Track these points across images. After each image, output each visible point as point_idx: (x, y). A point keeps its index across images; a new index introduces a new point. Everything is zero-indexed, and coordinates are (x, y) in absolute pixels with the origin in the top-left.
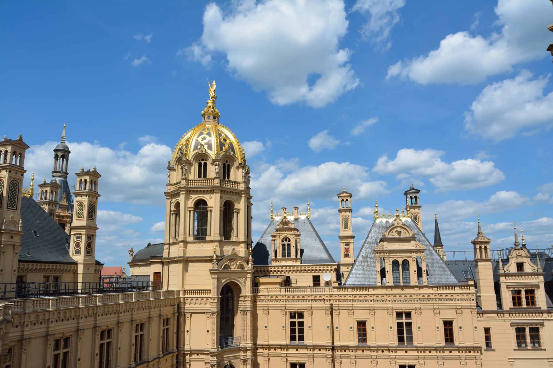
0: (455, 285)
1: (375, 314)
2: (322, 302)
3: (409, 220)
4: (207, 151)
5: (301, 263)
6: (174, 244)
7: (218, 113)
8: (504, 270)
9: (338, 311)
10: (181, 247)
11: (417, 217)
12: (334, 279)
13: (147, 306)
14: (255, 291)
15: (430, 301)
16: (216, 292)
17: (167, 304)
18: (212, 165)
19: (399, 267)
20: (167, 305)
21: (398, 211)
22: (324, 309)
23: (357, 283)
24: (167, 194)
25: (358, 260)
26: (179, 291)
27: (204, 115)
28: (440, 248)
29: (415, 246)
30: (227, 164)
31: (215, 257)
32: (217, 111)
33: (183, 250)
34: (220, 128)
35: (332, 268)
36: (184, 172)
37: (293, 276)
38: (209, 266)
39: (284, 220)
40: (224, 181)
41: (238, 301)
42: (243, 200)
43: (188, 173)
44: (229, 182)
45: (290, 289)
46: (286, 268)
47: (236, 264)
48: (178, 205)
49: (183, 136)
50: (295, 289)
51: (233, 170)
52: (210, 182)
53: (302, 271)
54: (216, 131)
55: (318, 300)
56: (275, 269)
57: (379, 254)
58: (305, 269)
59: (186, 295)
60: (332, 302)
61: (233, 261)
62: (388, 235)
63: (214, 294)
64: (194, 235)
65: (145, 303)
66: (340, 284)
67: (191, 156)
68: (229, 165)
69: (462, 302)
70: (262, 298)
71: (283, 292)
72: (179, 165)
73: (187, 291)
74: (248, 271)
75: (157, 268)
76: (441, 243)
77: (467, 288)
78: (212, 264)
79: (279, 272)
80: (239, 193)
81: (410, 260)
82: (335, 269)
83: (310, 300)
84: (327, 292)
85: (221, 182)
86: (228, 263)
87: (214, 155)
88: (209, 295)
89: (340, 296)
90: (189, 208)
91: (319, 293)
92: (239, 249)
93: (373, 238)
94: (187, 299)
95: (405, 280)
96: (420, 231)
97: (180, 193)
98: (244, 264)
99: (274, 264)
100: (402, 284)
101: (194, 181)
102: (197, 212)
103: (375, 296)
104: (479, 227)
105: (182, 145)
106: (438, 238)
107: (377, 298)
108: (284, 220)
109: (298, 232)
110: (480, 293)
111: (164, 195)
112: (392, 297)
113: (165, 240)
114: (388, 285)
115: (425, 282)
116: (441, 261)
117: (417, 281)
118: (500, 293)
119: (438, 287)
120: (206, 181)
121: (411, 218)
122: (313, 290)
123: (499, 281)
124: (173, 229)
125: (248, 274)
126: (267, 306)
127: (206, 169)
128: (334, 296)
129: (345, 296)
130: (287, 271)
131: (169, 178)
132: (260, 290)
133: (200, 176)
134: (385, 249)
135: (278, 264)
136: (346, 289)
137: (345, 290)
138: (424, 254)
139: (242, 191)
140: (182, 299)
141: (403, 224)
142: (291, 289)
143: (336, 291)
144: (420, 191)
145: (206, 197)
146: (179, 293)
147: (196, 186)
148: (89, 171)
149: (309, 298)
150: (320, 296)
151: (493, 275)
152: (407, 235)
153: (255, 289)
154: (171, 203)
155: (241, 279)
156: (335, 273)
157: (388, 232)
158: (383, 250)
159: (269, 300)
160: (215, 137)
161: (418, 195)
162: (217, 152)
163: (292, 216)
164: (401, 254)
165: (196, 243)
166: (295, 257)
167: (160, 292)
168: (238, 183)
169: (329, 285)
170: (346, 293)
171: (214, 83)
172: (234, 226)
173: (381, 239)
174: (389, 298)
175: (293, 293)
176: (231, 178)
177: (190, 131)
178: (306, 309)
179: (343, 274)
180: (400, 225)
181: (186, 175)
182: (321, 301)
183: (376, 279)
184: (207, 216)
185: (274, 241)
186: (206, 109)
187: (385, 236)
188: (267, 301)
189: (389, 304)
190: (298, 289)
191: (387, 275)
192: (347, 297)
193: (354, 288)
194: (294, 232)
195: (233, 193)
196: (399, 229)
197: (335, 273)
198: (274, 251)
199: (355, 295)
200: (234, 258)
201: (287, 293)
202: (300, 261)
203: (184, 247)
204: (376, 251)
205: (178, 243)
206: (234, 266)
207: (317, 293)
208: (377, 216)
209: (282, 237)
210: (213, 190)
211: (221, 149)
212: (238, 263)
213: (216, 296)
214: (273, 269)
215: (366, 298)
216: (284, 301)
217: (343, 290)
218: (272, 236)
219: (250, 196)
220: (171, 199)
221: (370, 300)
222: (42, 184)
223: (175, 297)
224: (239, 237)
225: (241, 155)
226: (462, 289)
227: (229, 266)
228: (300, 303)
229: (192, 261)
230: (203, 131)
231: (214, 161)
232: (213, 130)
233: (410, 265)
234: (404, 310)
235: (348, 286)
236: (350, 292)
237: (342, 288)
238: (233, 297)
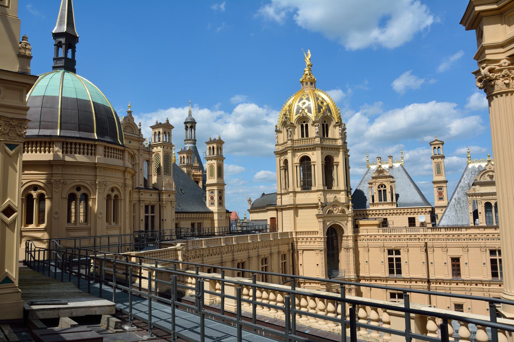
1: (468, 251)
2: (417, 241)
5: (397, 206)
6: (285, 194)
9: (432, 249)
10: (291, 197)
12: (429, 221)
14: (356, 231)
18: (313, 126)
21: (490, 156)
22: (419, 247)
23: (450, 224)
24: (276, 153)
25: (451, 203)
26: (292, 232)
27: (302, 82)
30: (325, 124)
31: (320, 204)
32: (313, 77)
35: (426, 211)
36: (290, 133)
37: (390, 218)
38: (316, 211)
39: (379, 169)
41: (342, 240)
42: (341, 154)
45: (387, 229)
46: (383, 211)
47: (338, 209)
48: (286, 162)
49: (286, 102)
50: (391, 230)
51: (331, 128)
52: (311, 141)
53: (398, 213)
54: (314, 96)
56: (373, 213)
57: (471, 197)
58: (401, 212)
60: (426, 241)
61: (335, 206)
63: (321, 235)
64: (301, 186)
66: (433, 225)
67: (294, 120)
68: (327, 125)
70: (362, 237)
73: (299, 232)
75: (273, 214)
79: (377, 215)
80: (337, 149)
82: (429, 211)
83: (406, 239)
84: (421, 231)
86: (331, 209)
89: (433, 235)
90: (295, 164)
91: (414, 233)
93: (466, 182)
94: (299, 239)
97: (287, 151)
99: (371, 208)
101: (298, 141)
103: (468, 235)
105: (286, 110)
107: (470, 237)
109: (393, 179)
112: (485, 236)
114: (480, 225)
120: (309, 140)
122: (409, 230)
125: (349, 218)
126: (367, 244)
130: (384, 214)
131: (277, 140)
132: (360, 230)
133: (303, 136)
134: (477, 192)
135: (375, 208)
136: (440, 229)
137: (439, 230)
139: (340, 146)
140: (295, 239)
142: (388, 230)
143: (429, 231)
145: (309, 154)
146: (292, 234)
147: (300, 145)
148: (215, 139)
149: (405, 238)
150: (415, 235)
153: (356, 230)
154: (280, 160)
156: (429, 215)
157: (480, 176)
158: (475, 194)
159: (369, 240)
160: (313, 101)
162: (316, 115)
166: (391, 201)
168: (336, 140)
169: (424, 226)
170: (439, 233)
171: (309, 52)
172: (335, 177)
173: (474, 183)
174: (482, 237)
175: (390, 233)
176: (330, 136)
177: (291, 98)
178: (402, 247)
179: (437, 215)
181: (291, 136)
182: (416, 240)
183: (468, 220)
185: (371, 187)
186: (304, 77)
187: (477, 180)
188: (367, 240)
189: (482, 243)
191: (480, 216)
192: (441, 237)
194: (389, 179)
196: (491, 173)
198: (371, 196)
199: (448, 235)
200: (336, 204)
201: (384, 233)
202: (396, 204)
203: (293, 197)
204: (468, 194)
205: (288, 193)
206: (337, 211)
207: (412, 233)
208: (470, 162)
209: (378, 184)
210: (315, 148)
211: (320, 111)
212: (340, 208)
213: (322, 236)
214: (371, 212)
215: (459, 237)
216: (382, 240)
217: (436, 230)
218: (368, 183)
219: (347, 149)
221: (463, 239)
222: (180, 152)
223: (289, 237)
225: (337, 115)
228: (396, 241)
229: (301, 208)
230: (303, 97)
231: (314, 122)
232: (311, 95)
234: (497, 248)
235: (442, 226)
236: (443, 231)
237: (436, 229)
238: (337, 237)
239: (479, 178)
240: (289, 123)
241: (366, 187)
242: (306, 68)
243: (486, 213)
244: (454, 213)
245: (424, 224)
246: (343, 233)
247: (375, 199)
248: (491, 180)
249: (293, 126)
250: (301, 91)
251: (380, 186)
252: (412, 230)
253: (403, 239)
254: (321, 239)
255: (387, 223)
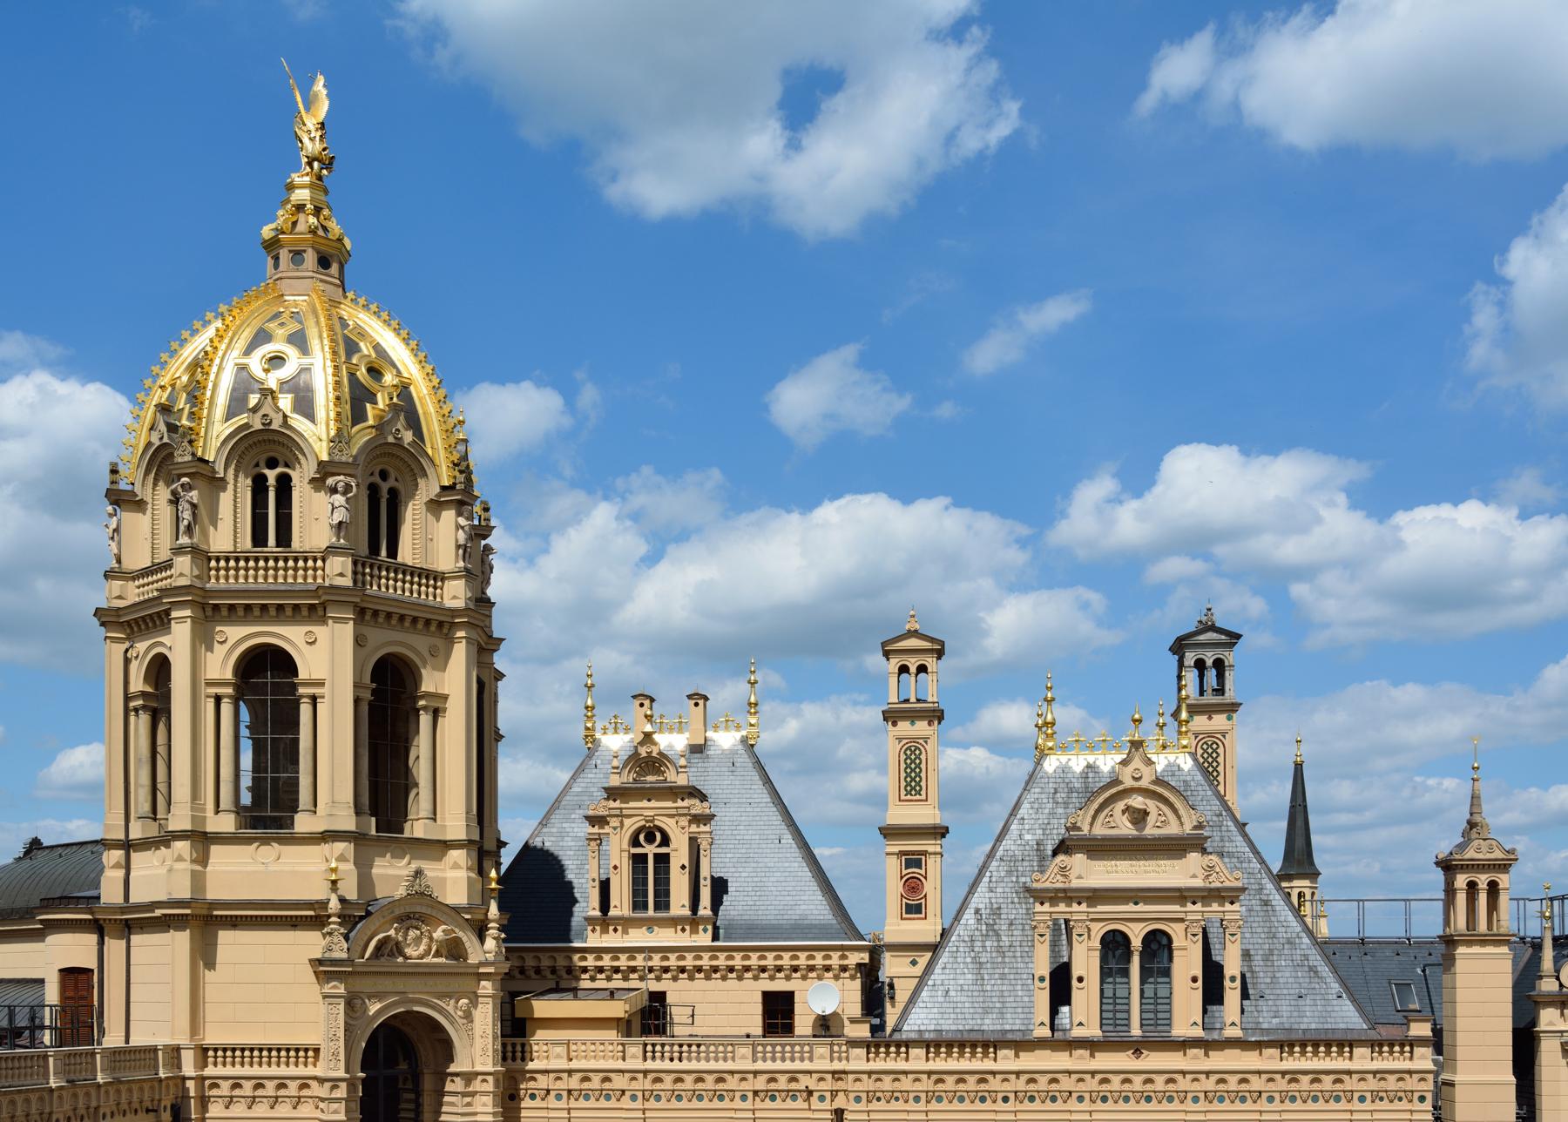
0: (1356, 1037)
2: (800, 1104)
3: (1186, 763)
4: (291, 422)
5: (715, 937)
6: (146, 844)
7: (340, 240)
8: (1558, 978)
10: (180, 859)
11: (1221, 751)
12: (855, 1009)
13: (33, 1111)
15: (1249, 1101)
16: (342, 1057)
17: (124, 1106)
18: (317, 490)
19: (1128, 961)
20: (125, 1107)
21: (1140, 721)
23: (950, 1025)
24: (108, 618)
25: (959, 930)
26: (177, 1050)
27: (272, 246)
28: (1307, 883)
29: (1201, 874)
30: (384, 487)
31: (334, 905)
32: (335, 228)
33: (192, 871)
34: (350, 315)
35: (845, 962)
36: (187, 515)
37: (677, 993)
38: (312, 943)
39: (643, 751)
40: (371, 567)
41: (441, 1093)
42: (460, 653)
43: (206, 520)
44: (396, 572)
45: (663, 1045)
46: (650, 958)
47: (431, 938)
48: (160, 669)
50: (685, 1048)
51: (413, 514)
52: (306, 569)
53: (715, 969)
54: (331, 328)
55: (784, 1094)
56: (600, 963)
57: (1047, 905)
58: (730, 963)
59: (211, 1067)
60: (840, 1102)
61: (415, 923)
62: (1092, 824)
63: (333, 1065)
64: (239, 809)
65: (27, 1101)
66: (876, 1029)
67: (215, 444)
68: (393, 493)
69: (1379, 1105)
70: (543, 1082)
71: (634, 1057)
72: (161, 484)
73: (216, 1050)
74: (482, 970)
75: (76, 949)
76: (1312, 863)
77: (1402, 1052)
78: (324, 936)
79: (619, 976)
80: (440, 625)
81: (1176, 932)
82: (859, 965)
83: (750, 1095)
84: (822, 1058)
85: (360, 568)
86: (392, 932)
87: (325, 444)
88: (310, 1067)
90: (210, 684)
91: (788, 1065)
92: (440, 874)
93: (1028, 837)
94: (216, 1086)
95: (1151, 1016)
96: (1228, 809)
97: (167, 612)
98: (465, 939)
99: (594, 939)
100: (1136, 1031)
101: (232, 563)
102: (248, 703)
103: (1024, 1078)
104: (1475, 799)
105: (173, 386)
106: (1300, 842)
107: (1032, 1087)
108: (643, 751)
109: (706, 804)
110: (1454, 1072)
111: (96, 622)
112: (1092, 1084)
113: (107, 828)
114: (1077, 1032)
115: (1233, 1024)
116: (1306, 940)
117: (1200, 1022)
118: (1533, 1075)
119: (1286, 1045)
120: (291, 563)
121: (1193, 755)
122: (764, 1052)
123: (1534, 1022)
124: (140, 776)
125: (483, 983)
127: (290, 507)
128: (851, 1077)
129: (898, 1080)
130: (651, 970)
131: (114, 545)
132: (535, 1048)
133: (259, 538)
134: (1075, 883)
135: (612, 940)
136: (903, 1049)
137: (898, 1053)
138: (1236, 907)
139: (454, 612)
140: (190, 1084)
141: (1158, 781)
142: (667, 1048)
143: (858, 1058)
144: (1238, 636)
145: (291, 637)
146: (179, 1058)
147: (244, 587)
149: (745, 1086)
150: (793, 1076)
151: (1510, 999)
152: (1173, 829)
153: (514, 1045)
154: (127, 661)
155: (452, 1002)
156: (857, 983)
157: (1092, 812)
158: (1064, 890)
159: (575, 1093)
160: (328, 356)
161: (1230, 657)
162: (339, 430)
163: (680, 731)
164: (1141, 907)
165: (248, 841)
166: (687, 912)
167: (93, 1054)
168: (438, 577)
169: (833, 1031)
170: (901, 1065)
171: (320, 86)
172: (422, 772)
173: (1062, 842)
174: (1081, 1087)
175: (676, 1061)
176: (406, 555)
177: (206, 323)
179: (891, 986)
180: (1145, 783)
181: (197, 530)
182: (794, 1098)
183: (1029, 1009)
184: (295, 725)
185: (599, 839)
186: (282, 216)
187: (1079, 829)
188: (565, 1094)
190: (699, 1046)
191: (1077, 995)
192: (906, 1083)
193: (935, 1045)
194: (686, 803)
195: (415, 620)
196: (1137, 801)
197: (858, 982)
198: (597, 883)
199: (939, 1076)
200: (418, 909)
201: (649, 1061)
202: (710, 927)
203: (193, 861)
204: (1036, 890)
205: (165, 840)
206: (422, 948)
207: (779, 1065)
208: (1050, 744)
209: (631, 825)
210: (324, 605)
212: (438, 934)
213: (341, 1073)
214: (590, 961)
215: (983, 1087)
216: (640, 1094)
217: (888, 1053)
218: (587, 818)
220: (128, 639)
221: (1000, 1096)
223: (162, 1074)
224: (443, 819)
225: (449, 449)
226: (1381, 1053)
227: (397, 943)
228: (705, 1104)
229: (235, 923)
230: (272, 325)
231: (325, 470)
232: (318, 323)
233: (1176, 953)
235: (913, 1036)
236: (917, 1060)
237: (888, 1046)
238: (416, 1077)
239: (1089, 819)
240: (188, 458)
241: (576, 838)
242: (297, 169)
243: (1102, 982)
244: (970, 976)
245: (830, 1023)
246: (450, 1058)
247: (614, 901)
248: (1135, 833)
249: (207, 477)
250: (265, 293)
251: (642, 837)
252: (778, 1048)
253: (738, 1095)
254: (336, 1087)
255: (665, 1018)
